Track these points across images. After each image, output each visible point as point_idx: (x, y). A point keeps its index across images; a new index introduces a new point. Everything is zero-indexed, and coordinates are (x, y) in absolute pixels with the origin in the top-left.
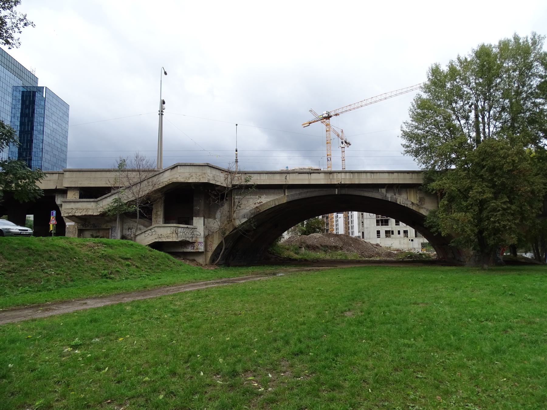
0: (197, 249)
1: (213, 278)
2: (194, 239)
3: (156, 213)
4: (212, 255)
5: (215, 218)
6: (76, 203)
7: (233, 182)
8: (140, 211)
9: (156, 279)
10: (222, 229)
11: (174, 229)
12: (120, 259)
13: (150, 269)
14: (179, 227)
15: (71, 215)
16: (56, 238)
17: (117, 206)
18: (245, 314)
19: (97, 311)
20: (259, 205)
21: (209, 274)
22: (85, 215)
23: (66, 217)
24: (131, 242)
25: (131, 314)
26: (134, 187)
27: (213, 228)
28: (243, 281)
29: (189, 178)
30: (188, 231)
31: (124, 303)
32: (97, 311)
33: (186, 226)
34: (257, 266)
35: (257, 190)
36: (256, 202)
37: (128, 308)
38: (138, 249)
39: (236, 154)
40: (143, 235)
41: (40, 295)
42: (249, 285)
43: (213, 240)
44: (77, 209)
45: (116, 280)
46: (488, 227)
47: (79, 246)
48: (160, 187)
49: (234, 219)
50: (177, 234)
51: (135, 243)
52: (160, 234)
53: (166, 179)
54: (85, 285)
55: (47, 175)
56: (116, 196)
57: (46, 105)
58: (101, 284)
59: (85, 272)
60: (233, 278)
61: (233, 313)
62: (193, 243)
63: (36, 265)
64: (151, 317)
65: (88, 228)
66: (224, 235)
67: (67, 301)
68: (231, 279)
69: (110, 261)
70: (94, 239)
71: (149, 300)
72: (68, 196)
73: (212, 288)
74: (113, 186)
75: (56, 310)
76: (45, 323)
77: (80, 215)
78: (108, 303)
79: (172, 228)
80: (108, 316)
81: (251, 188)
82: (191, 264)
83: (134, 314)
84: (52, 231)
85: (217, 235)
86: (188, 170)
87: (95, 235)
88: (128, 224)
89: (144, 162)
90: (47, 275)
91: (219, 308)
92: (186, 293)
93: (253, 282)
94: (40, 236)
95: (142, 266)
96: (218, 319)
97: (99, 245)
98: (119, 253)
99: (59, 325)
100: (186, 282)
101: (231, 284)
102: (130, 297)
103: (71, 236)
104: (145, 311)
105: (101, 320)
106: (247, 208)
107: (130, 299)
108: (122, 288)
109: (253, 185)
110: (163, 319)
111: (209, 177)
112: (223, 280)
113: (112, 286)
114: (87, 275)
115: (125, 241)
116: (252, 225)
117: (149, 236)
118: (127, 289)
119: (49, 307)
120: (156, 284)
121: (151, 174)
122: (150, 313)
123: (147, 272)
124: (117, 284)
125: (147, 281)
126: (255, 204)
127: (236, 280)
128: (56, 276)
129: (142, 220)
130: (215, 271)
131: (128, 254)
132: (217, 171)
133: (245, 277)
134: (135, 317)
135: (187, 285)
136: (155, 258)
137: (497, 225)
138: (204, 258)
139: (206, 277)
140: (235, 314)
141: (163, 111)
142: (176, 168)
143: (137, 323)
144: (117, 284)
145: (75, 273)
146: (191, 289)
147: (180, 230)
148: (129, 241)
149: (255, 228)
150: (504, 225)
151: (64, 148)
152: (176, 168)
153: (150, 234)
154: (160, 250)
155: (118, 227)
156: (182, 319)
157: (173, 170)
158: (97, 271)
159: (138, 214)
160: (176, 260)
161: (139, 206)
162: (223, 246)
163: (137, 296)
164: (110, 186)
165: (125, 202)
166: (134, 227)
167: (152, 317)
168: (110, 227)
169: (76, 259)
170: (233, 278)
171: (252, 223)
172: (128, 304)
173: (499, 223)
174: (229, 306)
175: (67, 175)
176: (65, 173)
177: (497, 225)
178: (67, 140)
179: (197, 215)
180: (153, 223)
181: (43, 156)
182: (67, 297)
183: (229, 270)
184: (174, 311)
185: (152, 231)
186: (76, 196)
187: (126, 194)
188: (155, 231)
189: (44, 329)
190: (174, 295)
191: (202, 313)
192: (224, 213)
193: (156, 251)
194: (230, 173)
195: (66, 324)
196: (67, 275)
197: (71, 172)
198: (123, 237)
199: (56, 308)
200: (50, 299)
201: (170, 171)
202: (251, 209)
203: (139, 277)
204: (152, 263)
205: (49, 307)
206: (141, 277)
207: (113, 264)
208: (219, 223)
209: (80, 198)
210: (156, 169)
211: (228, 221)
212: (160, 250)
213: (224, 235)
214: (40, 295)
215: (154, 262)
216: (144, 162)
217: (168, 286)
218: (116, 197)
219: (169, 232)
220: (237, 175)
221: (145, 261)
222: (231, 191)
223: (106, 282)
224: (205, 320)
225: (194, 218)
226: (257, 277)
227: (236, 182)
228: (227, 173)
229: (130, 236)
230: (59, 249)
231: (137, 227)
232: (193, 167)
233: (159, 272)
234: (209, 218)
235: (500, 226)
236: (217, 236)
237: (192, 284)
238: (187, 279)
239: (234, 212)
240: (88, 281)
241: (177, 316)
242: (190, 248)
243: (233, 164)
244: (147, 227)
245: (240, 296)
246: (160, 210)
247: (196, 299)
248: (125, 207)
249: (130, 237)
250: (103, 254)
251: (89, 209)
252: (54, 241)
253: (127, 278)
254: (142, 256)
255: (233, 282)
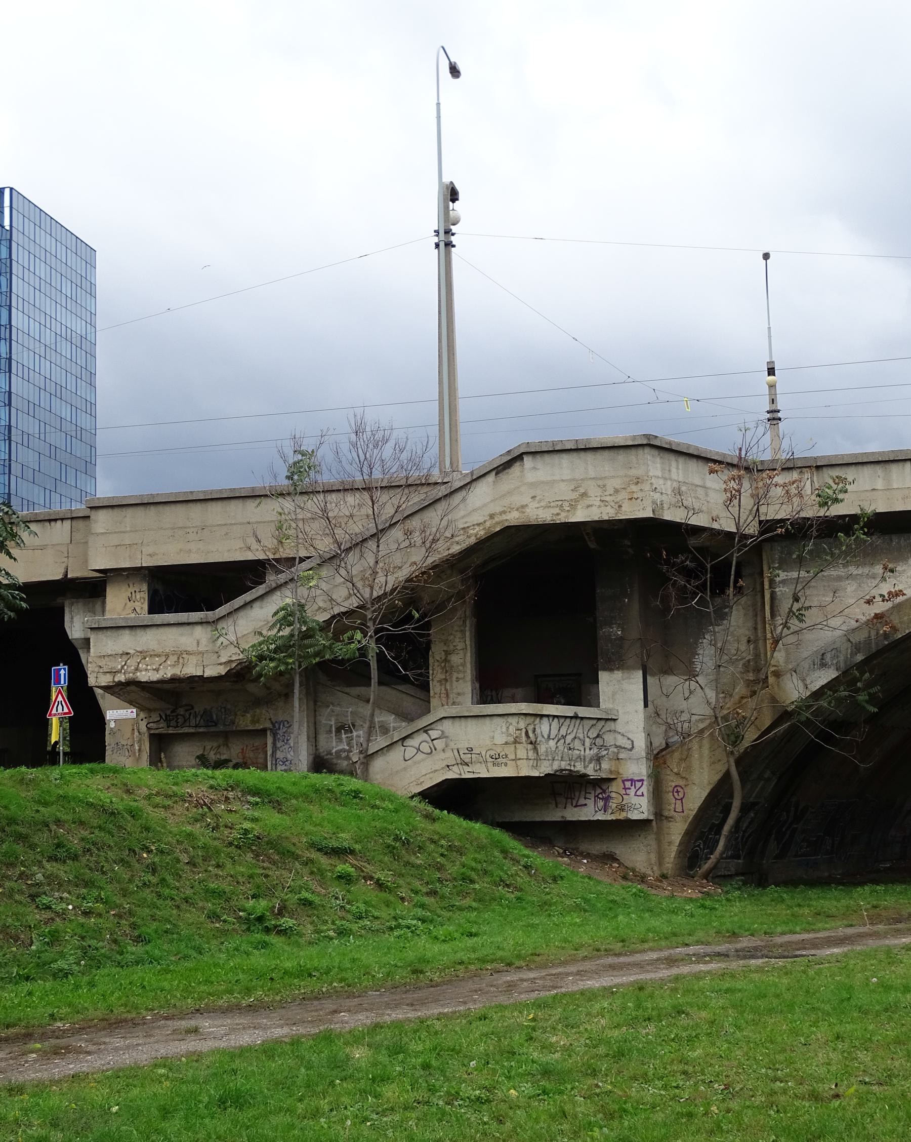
1: (700, 934)
2: (605, 765)
3: (446, 660)
4: (688, 833)
5: (692, 675)
6: (140, 632)
7: (763, 509)
8: (380, 656)
9: (456, 935)
10: (725, 718)
11: (522, 725)
12: (314, 855)
13: (433, 893)
14: (542, 716)
15: (121, 678)
16: (74, 769)
17: (292, 635)
18: (862, 1101)
19: (237, 1064)
20: (889, 605)
21: (679, 919)
22: (174, 680)
23: (106, 688)
24: (354, 783)
25: (373, 1080)
26: (352, 557)
27: (685, 717)
28: (836, 950)
29: (573, 507)
30: (579, 730)
31: (340, 1035)
32: (237, 1064)
33: (569, 710)
34: (894, 882)
35: (877, 540)
36: (875, 592)
37: (359, 1054)
38: (381, 813)
39: (772, 386)
40: (396, 755)
41: (30, 994)
42: (864, 969)
43: (689, 768)
44: (143, 654)
45: (302, 941)
47: (158, 799)
48: (456, 549)
49: (777, 674)
50: (534, 744)
51: (368, 785)
52: (463, 745)
54: (186, 957)
55: (33, 527)
56: (284, 599)
57: (14, 257)
58: (247, 954)
59: (184, 906)
60: (786, 938)
61: (804, 1089)
62: (600, 785)
63: (9, 878)
64: (452, 1097)
65: (186, 730)
66: (734, 744)
67: (125, 1021)
68: (779, 940)
69: (274, 863)
70: (210, 772)
71: (438, 1025)
72: (109, 605)
73: (698, 977)
74: (271, 557)
75: (89, 1053)
76: (54, 1101)
77: (155, 677)
78: (278, 1032)
79: (513, 720)
80: (283, 1084)
81: (848, 531)
82: (598, 874)
83: (384, 1079)
84: (56, 743)
85: (706, 744)
87: (212, 757)
88: (337, 709)
89: (388, 451)
90: (48, 915)
91: (740, 1065)
92: (590, 996)
93: (882, 956)
94: (15, 765)
95: (401, 882)
96: (739, 1114)
97: (231, 795)
98: (308, 827)
99: (105, 1112)
100: (582, 953)
101: (781, 962)
102: (359, 1009)
103: (128, 763)
104: (426, 1066)
105: (259, 1098)
106: (835, 622)
107: (363, 1020)
108: (327, 972)
109: (854, 518)
110: (503, 1106)
111: (657, 496)
112: (745, 942)
113: (288, 965)
114: (191, 916)
115: (327, 780)
116: (862, 697)
117: (420, 756)
118: (349, 975)
119: (63, 1042)
120: (460, 955)
121: (416, 499)
122: (447, 1080)
123: (423, 906)
124: (307, 956)
125: (424, 946)
126: (869, 602)
127: (803, 945)
128: (82, 920)
129: (390, 693)
130: (703, 906)
131: (343, 831)
132: (693, 465)
133: (842, 931)
134: (390, 1092)
135: (588, 965)
136: (450, 848)
138: (653, 844)
139: (667, 929)
140: (815, 1096)
141: (454, 229)
142: (518, 464)
143: (397, 1117)
144: (307, 956)
145: (147, 911)
146: (606, 981)
147: (544, 727)
148: (345, 779)
149: (873, 709)
151: (84, 421)
152: (516, 468)
153: (425, 747)
154: (468, 817)
155: (301, 725)
156: (582, 1107)
158: (228, 900)
159: (374, 665)
160: (538, 858)
161: (377, 631)
162: (731, 796)
163: (388, 1006)
164: (261, 556)
165: (323, 617)
166: (359, 722)
167: (457, 1096)
168: (269, 725)
169: (149, 852)
170: (786, 938)
171: (857, 691)
172: (356, 1039)
174: (780, 1057)
175: (102, 520)
176: (94, 515)
178: (92, 385)
179: (616, 663)
180: (434, 702)
181: (13, 457)
182: (126, 1005)
183: (765, 899)
184: (546, 1072)
185: (434, 734)
186: (137, 605)
187: (324, 586)
188: (443, 736)
189: (55, 1125)
190: (539, 1005)
191: (665, 1087)
192: (732, 648)
193: (453, 817)
194: (747, 469)
195: (133, 1112)
196: (119, 916)
197: (116, 512)
198: (320, 764)
199: (91, 1048)
200: (65, 1010)
201: (491, 478)
202: (854, 624)
203: (391, 929)
204: (440, 868)
205: (63, 1042)
206: (398, 926)
207: (285, 873)
208: (711, 694)
209: (151, 611)
210: (436, 476)
211: (749, 683)
212: (469, 814)
213: (734, 744)
214: (30, 994)
215: (448, 866)
216: (388, 451)
217: (509, 964)
218: (289, 601)
219: (500, 739)
220: (780, 479)
221: (413, 859)
222: (758, 549)
223: (265, 945)
224: (680, 1115)
226: (898, 931)
227: (776, 511)
228: (735, 472)
229: (348, 758)
230: (87, 815)
231: (372, 721)
232: (589, 456)
233: (471, 908)
234: (667, 671)
236: (706, 752)
237: (611, 960)
238: (586, 939)
239: (776, 642)
240: (198, 941)
241: (561, 1093)
242: (590, 803)
243: (761, 429)
244: (408, 718)
245: (829, 1014)
246: (460, 646)
247: (633, 1022)
248: (322, 641)
249: (344, 764)
250: (246, 832)
251: (188, 653)
252: (68, 783)
253: (342, 933)
254: (397, 838)
255: (789, 952)
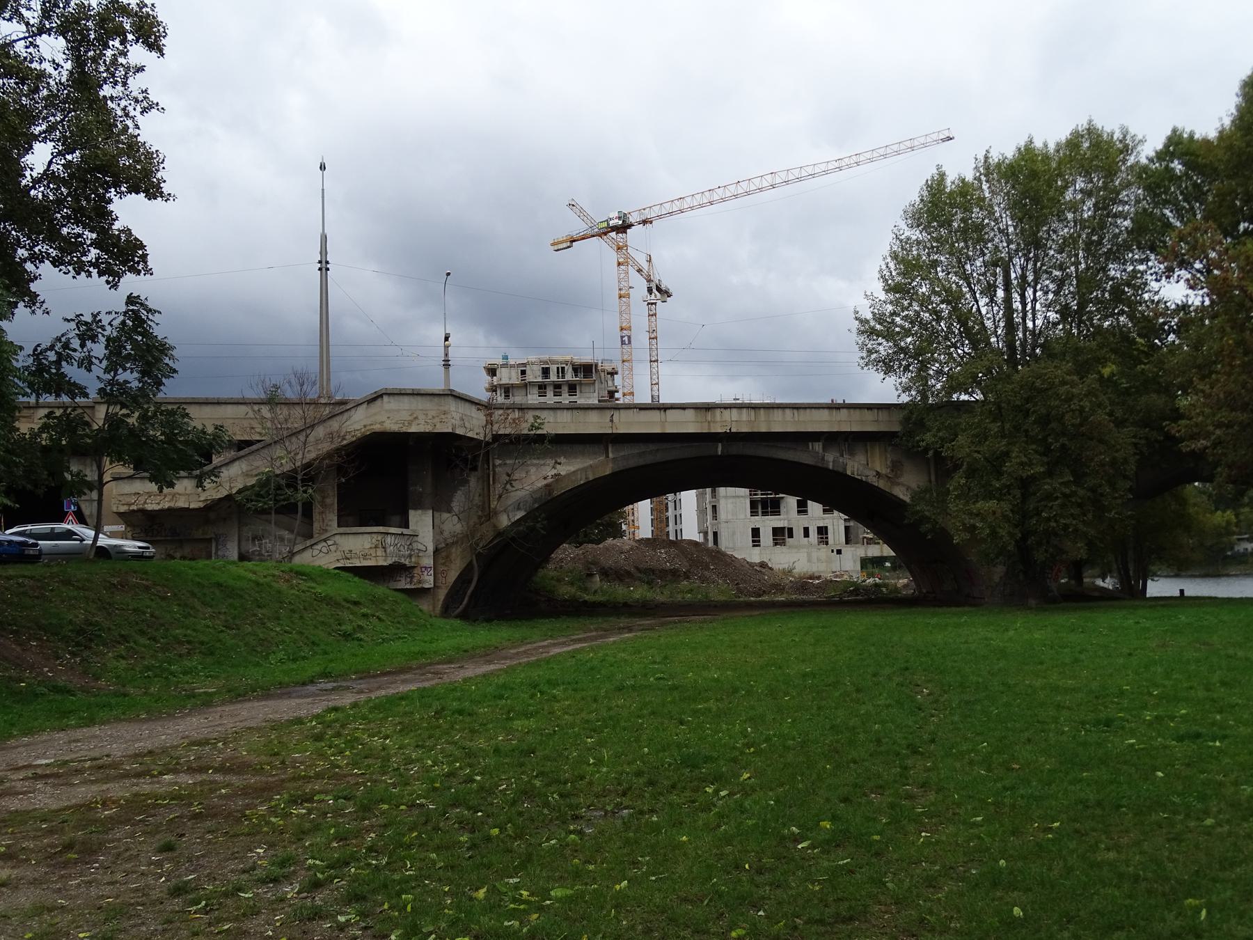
0: (420, 582)
2: (413, 560)
46: (1037, 529)
52: (346, 549)
53: (359, 423)
86: (406, 404)
117: (321, 554)
137: (1053, 524)
142: (380, 399)
150: (1065, 524)
152: (378, 402)
153: (324, 550)
157: (372, 405)
173: (1056, 521)
177: (1053, 524)
179: (419, 506)
185: (330, 542)
201: (365, 406)
225: (410, 511)
235: (1058, 526)
